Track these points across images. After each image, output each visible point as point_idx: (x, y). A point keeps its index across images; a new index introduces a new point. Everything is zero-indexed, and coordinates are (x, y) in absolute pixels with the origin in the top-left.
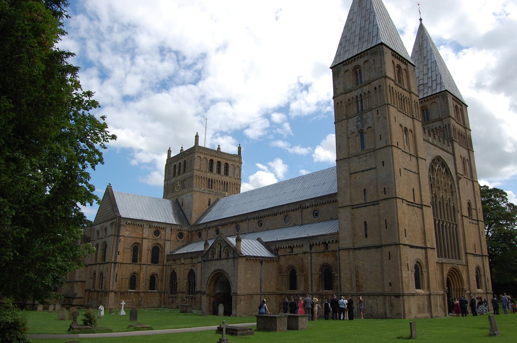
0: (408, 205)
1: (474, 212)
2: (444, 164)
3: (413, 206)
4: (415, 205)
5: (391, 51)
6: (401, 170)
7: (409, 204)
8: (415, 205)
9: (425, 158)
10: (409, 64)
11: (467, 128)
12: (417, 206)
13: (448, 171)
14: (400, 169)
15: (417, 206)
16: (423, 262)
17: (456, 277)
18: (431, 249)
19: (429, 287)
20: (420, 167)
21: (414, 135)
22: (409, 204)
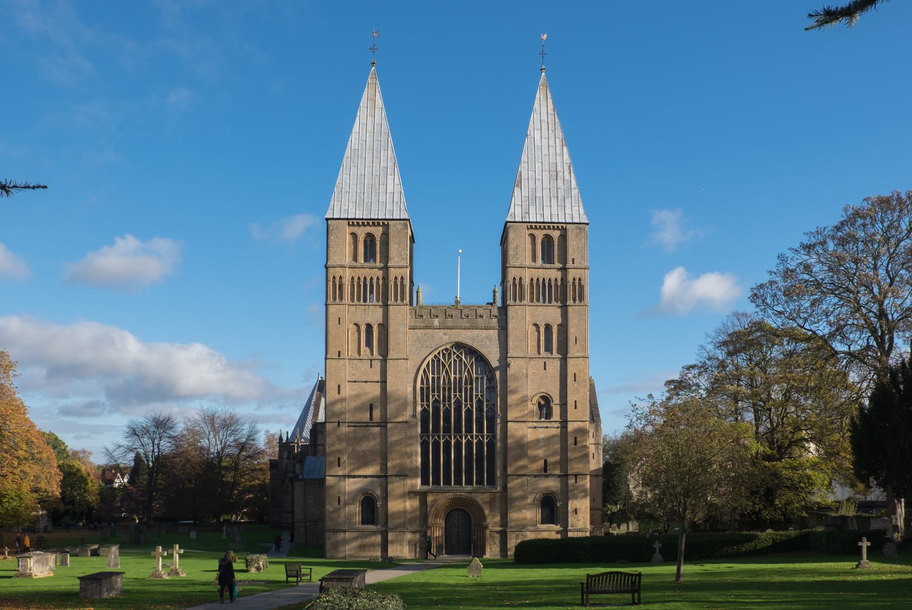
0: (355, 426)
1: (556, 411)
2: (471, 352)
3: (367, 426)
4: (371, 424)
5: (346, 222)
6: (341, 386)
7: (357, 425)
8: (371, 424)
9: (406, 357)
10: (390, 222)
11: (568, 268)
12: (376, 425)
13: (481, 359)
14: (339, 386)
15: (376, 425)
16: (378, 492)
17: (473, 508)
18: (398, 477)
19: (386, 523)
20: (389, 372)
21: (386, 330)
22: (357, 425)
